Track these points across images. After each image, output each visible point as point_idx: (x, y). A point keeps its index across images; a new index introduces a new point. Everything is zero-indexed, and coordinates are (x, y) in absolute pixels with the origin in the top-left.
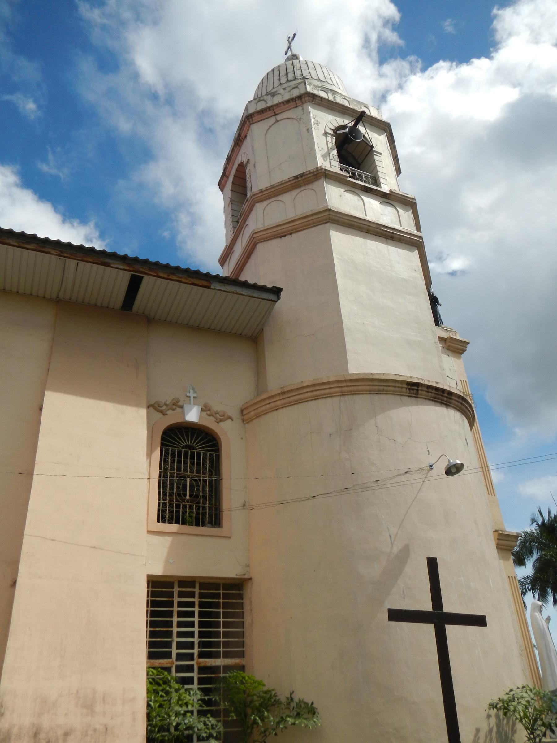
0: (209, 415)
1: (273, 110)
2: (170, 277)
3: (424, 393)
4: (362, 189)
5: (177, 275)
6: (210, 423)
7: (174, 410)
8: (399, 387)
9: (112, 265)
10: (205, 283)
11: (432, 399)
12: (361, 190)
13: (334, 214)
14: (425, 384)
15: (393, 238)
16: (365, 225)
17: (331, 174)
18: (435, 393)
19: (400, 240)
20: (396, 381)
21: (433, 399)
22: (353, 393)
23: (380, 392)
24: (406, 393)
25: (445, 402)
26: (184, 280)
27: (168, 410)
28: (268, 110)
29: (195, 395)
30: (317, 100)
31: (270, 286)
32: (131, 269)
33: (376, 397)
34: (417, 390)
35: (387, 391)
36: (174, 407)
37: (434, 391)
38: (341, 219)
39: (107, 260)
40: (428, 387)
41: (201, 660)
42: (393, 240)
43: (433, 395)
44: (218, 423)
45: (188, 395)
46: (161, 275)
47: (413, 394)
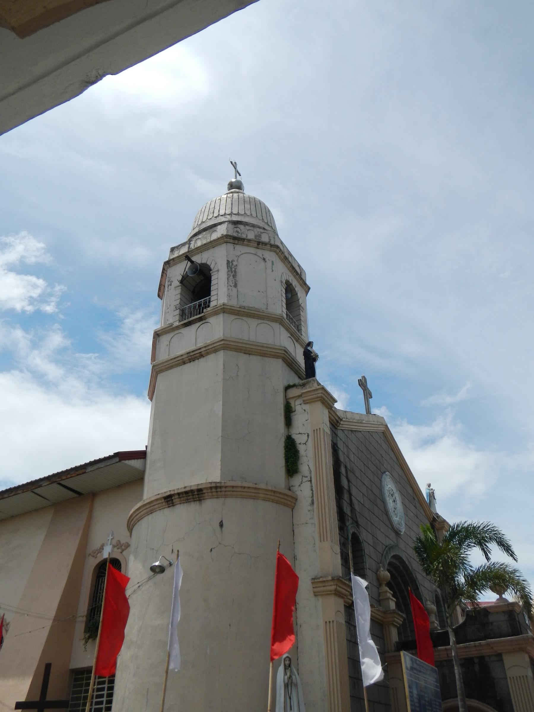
0: (118, 549)
1: (162, 284)
2: (67, 477)
3: (177, 500)
4: (185, 326)
7: (100, 552)
8: (160, 503)
9: (43, 485)
10: (83, 471)
11: (184, 501)
12: (184, 327)
13: (158, 367)
14: (175, 494)
15: (203, 355)
16: (179, 360)
17: (160, 332)
18: (186, 496)
19: (208, 353)
20: (157, 500)
21: (186, 501)
22: (141, 518)
23: (152, 512)
24: (166, 505)
25: (198, 499)
27: (98, 553)
28: (160, 286)
29: (112, 538)
32: (50, 482)
33: (150, 517)
34: (172, 500)
35: (155, 509)
36: (101, 550)
37: (184, 495)
38: (163, 368)
39: (41, 483)
40: (179, 494)
42: (204, 357)
43: (185, 498)
45: (108, 539)
46: (64, 478)
47: (171, 504)
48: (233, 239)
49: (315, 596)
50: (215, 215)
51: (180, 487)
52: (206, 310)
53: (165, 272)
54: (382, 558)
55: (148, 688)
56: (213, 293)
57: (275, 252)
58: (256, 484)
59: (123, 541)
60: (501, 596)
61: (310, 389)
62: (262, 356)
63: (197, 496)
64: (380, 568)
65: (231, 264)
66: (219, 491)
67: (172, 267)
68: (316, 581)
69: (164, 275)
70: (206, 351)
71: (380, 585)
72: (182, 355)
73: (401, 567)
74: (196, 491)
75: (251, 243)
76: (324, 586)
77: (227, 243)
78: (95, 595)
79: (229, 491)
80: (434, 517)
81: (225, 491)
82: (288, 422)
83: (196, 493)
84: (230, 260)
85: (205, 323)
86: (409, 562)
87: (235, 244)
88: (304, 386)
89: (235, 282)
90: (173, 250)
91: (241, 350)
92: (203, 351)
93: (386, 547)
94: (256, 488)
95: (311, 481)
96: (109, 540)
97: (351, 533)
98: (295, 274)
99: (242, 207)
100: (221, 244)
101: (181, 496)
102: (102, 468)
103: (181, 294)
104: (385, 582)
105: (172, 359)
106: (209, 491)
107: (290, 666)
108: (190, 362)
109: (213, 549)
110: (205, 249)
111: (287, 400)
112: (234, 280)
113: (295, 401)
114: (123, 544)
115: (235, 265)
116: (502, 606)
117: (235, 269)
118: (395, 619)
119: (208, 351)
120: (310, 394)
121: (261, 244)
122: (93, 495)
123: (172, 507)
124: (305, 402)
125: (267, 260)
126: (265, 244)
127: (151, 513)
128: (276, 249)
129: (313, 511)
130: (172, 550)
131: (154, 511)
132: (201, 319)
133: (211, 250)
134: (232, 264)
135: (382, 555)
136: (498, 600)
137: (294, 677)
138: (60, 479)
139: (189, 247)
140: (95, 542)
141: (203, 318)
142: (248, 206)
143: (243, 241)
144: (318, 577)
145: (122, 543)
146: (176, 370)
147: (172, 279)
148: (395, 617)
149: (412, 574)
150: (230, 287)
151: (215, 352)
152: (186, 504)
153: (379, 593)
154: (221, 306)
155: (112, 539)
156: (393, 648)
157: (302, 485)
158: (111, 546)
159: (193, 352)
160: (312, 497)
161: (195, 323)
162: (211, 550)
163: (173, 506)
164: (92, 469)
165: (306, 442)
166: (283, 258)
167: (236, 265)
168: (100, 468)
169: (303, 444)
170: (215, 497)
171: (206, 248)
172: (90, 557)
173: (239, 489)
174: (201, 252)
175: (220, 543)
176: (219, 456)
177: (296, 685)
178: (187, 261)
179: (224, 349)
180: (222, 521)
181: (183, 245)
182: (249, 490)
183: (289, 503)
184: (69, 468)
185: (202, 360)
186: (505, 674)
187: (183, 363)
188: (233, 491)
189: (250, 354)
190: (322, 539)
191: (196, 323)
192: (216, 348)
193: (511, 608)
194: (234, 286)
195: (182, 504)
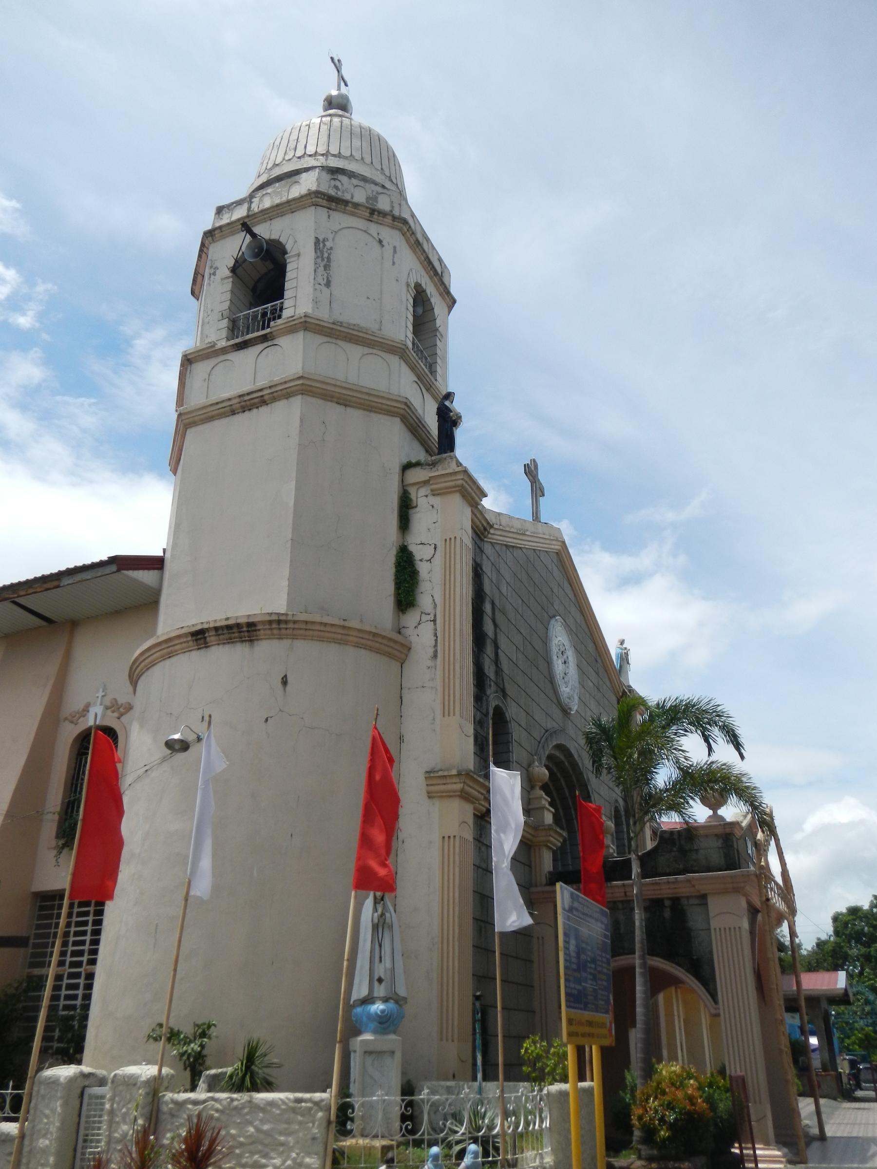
0: (113, 712)
2: (29, 592)
3: (213, 638)
5: (34, 586)
6: (111, 721)
7: (84, 716)
8: (185, 642)
10: (55, 583)
11: (226, 641)
12: (236, 351)
13: (186, 417)
14: (210, 628)
18: (229, 633)
20: (179, 637)
24: (194, 646)
26: (39, 590)
27: (79, 718)
29: (103, 694)
30: (217, 236)
31: (105, 558)
33: (168, 662)
34: (205, 638)
35: (176, 651)
36: (85, 713)
37: (225, 631)
40: (216, 629)
41: (89, 967)
42: (267, 404)
44: (119, 718)
45: (97, 695)
46: (22, 593)
47: (202, 644)
48: (327, 200)
49: (429, 797)
50: (299, 154)
51: (218, 618)
52: (275, 323)
53: (205, 250)
54: (538, 746)
55: (157, 925)
56: (287, 294)
57: (400, 230)
58: (344, 620)
59: (121, 700)
60: (715, 812)
61: (444, 472)
62: (368, 410)
63: (246, 634)
64: (534, 762)
65: (321, 245)
66: (284, 628)
67: (218, 243)
68: (432, 775)
69: (204, 255)
70: (271, 395)
71: (532, 787)
72: (230, 399)
73: (566, 763)
74: (244, 626)
75: (358, 209)
76: (445, 784)
77: (317, 207)
78: (74, 782)
79: (301, 629)
80: (624, 690)
81: (293, 629)
82: (404, 522)
83: (245, 629)
84: (321, 239)
85: (273, 345)
86: (579, 756)
87: (331, 210)
88: (434, 466)
89: (328, 278)
90: (220, 210)
91: (332, 397)
92: (265, 395)
93: (547, 731)
94: (344, 627)
95: (434, 621)
96: (98, 697)
97: (494, 706)
98: (433, 275)
99: (346, 144)
100: (306, 208)
101: (220, 632)
102: (89, 579)
103: (232, 292)
104: (541, 784)
105: (212, 405)
106: (267, 627)
107: (382, 899)
108: (244, 411)
109: (269, 719)
110: (278, 214)
111: (405, 488)
112: (326, 275)
113: (418, 489)
114: (122, 704)
115: (329, 248)
116: (715, 826)
117: (329, 254)
118: (552, 839)
119: (275, 394)
120: (443, 480)
121: (376, 213)
122: (74, 624)
123: (204, 649)
124: (435, 493)
125: (385, 243)
126: (383, 214)
127: (170, 657)
128: (402, 225)
129: (435, 669)
130: (203, 717)
131: (175, 654)
132: (265, 339)
133: (287, 216)
134: (324, 245)
135: (539, 742)
136: (710, 817)
137: (388, 915)
138: (16, 595)
139: (249, 209)
140: (74, 701)
141: (268, 336)
142: (357, 143)
143: (346, 206)
144: (435, 770)
145: (120, 702)
146: (217, 423)
147: (217, 264)
148: (550, 836)
149: (581, 774)
150: (318, 286)
151: (287, 398)
152: (227, 646)
153: (530, 799)
154: (301, 318)
155: (103, 696)
156: (544, 881)
157: (420, 627)
158: (102, 707)
159: (248, 394)
160: (436, 646)
161: (254, 345)
162: (267, 720)
163: (206, 647)
164: (70, 582)
165: (432, 558)
166: (413, 242)
167: (331, 248)
168: (85, 580)
169: (426, 560)
170: (276, 637)
171: (279, 211)
172: (67, 723)
173: (317, 627)
174: (271, 219)
175: (280, 710)
176: (287, 572)
177: (391, 927)
178: (245, 232)
179: (302, 394)
180: (286, 676)
181: (239, 203)
182: (333, 630)
183: (397, 653)
184: (31, 577)
185: (264, 410)
186: (709, 924)
187: (232, 412)
188: (306, 629)
189: (346, 406)
190: (446, 713)
191: (256, 344)
192: (288, 390)
193: (728, 830)
194: (325, 285)
195: (221, 646)
